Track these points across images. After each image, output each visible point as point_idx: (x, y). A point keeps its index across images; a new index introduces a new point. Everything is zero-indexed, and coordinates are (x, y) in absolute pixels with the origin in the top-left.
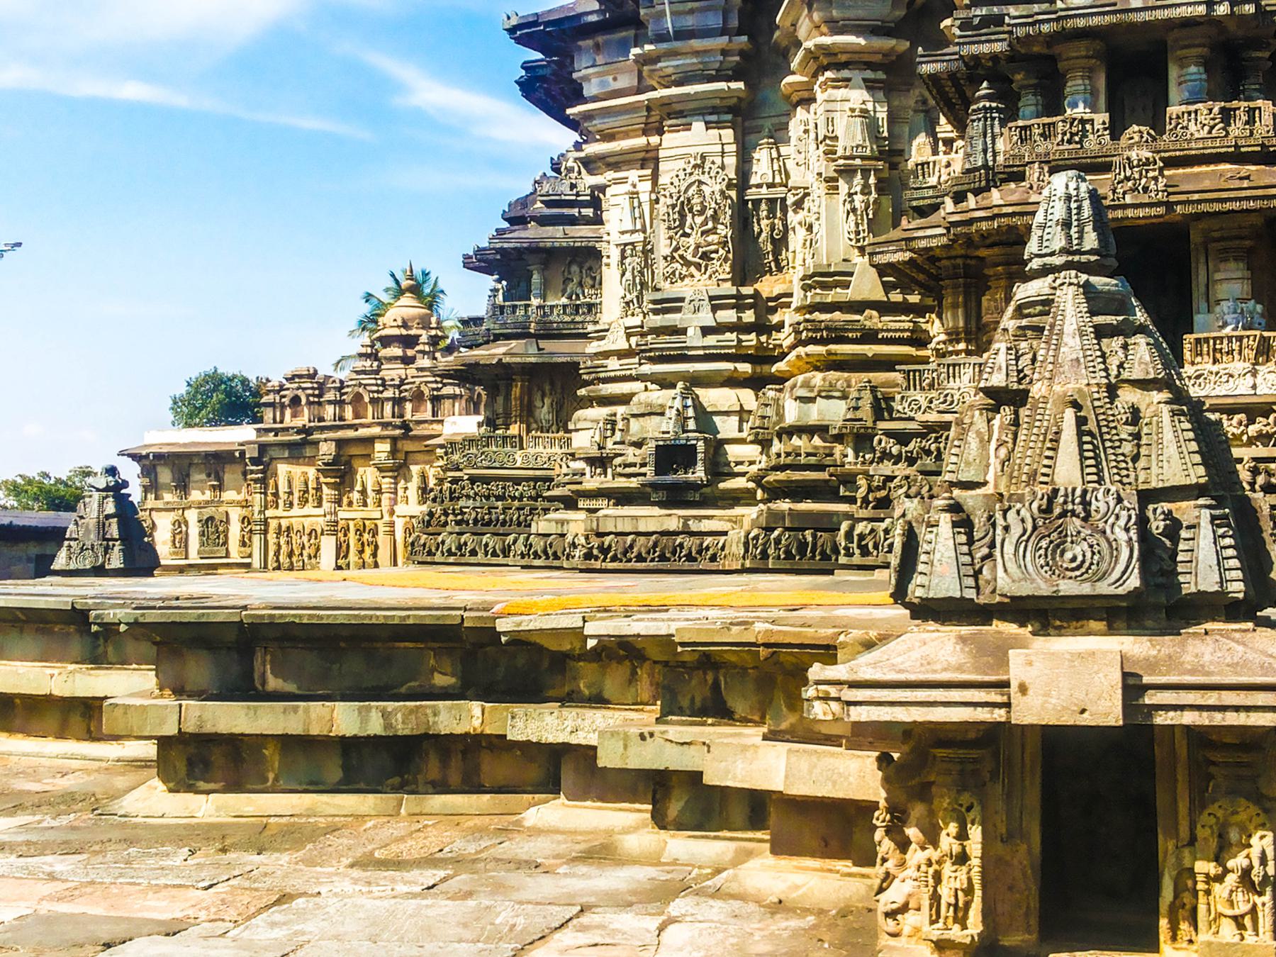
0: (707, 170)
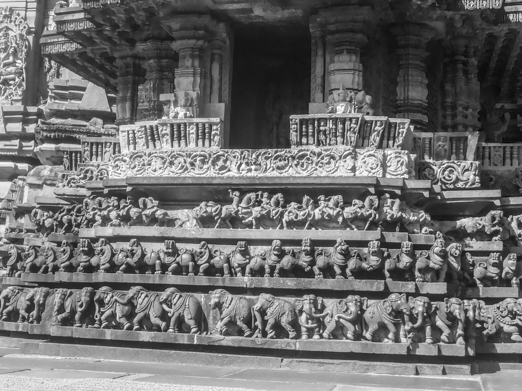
0: (13, 19)
